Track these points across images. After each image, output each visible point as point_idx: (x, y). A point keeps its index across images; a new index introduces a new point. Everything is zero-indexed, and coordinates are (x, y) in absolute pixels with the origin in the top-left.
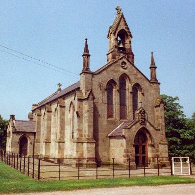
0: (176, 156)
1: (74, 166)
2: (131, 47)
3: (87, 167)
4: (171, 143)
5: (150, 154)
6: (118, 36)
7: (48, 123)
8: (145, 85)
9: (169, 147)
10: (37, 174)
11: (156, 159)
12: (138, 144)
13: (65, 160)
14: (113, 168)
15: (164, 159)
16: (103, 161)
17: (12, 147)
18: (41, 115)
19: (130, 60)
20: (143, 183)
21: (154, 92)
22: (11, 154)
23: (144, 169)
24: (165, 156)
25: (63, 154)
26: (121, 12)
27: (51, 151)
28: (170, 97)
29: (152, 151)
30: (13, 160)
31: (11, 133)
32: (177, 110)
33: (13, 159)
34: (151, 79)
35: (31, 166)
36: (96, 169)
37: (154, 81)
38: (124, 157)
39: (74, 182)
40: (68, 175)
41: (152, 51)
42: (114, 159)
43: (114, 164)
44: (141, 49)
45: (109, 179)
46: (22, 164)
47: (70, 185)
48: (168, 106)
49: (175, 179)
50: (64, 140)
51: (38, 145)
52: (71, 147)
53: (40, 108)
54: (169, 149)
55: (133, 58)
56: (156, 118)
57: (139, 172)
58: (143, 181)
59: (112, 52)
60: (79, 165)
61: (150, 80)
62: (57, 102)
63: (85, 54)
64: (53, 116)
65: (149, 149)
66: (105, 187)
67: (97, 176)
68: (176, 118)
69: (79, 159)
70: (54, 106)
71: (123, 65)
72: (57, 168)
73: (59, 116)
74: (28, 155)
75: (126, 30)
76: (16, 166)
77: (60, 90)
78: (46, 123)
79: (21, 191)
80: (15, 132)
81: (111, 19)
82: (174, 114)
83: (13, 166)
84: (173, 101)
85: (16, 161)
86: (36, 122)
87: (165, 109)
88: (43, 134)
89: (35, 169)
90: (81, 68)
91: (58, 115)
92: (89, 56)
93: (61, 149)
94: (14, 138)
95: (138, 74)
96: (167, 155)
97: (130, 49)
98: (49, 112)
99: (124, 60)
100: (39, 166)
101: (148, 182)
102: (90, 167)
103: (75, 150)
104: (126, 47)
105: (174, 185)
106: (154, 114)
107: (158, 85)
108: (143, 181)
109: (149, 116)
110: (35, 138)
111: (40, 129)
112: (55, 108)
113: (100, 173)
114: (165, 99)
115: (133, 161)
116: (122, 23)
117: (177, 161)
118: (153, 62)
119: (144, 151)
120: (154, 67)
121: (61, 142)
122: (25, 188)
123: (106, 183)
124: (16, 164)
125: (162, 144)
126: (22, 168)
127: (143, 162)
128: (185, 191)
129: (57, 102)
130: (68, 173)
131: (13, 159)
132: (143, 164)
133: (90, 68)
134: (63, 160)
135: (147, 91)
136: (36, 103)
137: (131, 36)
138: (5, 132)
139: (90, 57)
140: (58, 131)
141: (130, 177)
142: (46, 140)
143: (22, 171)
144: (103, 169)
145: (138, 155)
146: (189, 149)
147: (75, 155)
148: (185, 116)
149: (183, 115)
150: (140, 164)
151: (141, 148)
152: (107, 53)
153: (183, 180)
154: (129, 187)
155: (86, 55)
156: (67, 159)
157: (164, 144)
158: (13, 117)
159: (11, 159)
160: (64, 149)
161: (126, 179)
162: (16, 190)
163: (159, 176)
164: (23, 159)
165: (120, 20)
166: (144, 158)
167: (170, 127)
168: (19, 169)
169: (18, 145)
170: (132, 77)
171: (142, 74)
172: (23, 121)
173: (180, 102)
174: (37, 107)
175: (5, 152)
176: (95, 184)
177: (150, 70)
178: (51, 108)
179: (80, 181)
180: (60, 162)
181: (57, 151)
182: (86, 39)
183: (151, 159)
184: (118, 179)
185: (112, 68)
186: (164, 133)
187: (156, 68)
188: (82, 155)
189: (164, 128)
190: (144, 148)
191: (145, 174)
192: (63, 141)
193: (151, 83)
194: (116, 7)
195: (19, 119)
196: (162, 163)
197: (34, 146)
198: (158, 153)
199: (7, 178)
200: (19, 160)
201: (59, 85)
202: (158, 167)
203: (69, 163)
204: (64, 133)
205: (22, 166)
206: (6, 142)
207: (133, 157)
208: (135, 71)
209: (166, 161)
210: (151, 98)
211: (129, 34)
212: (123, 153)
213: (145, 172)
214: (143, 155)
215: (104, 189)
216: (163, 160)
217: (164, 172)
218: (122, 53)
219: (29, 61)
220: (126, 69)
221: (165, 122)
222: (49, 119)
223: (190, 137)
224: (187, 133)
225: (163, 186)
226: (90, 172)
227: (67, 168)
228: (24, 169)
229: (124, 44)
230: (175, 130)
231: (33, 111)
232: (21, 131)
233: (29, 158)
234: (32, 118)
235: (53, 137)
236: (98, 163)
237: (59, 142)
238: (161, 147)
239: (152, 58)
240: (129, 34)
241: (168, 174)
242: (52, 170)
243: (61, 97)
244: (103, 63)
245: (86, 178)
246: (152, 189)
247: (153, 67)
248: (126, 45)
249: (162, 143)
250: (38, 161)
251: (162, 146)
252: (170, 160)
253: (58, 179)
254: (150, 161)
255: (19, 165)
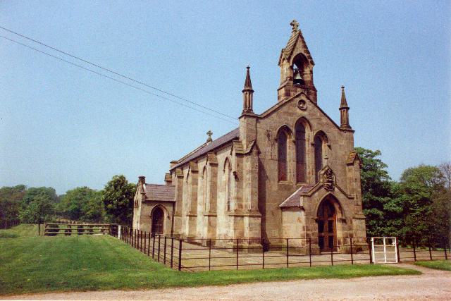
0: (377, 236)
1: (231, 250)
2: (312, 78)
3: (249, 252)
4: (369, 218)
5: (339, 233)
6: (293, 63)
7: (193, 189)
8: (332, 133)
9: (367, 222)
10: (178, 262)
11: (349, 240)
12: (322, 219)
13: (217, 241)
14: (286, 252)
15: (360, 240)
16: (273, 242)
17: (141, 223)
18: (183, 177)
19: (311, 97)
20: (329, 274)
21: (346, 144)
22: (140, 233)
23: (332, 254)
24: (361, 236)
25: (214, 233)
26: (299, 28)
27: (197, 229)
28: (368, 151)
29: (343, 229)
30: (143, 242)
31: (140, 203)
32: (378, 169)
33: (143, 240)
34: (341, 125)
35: (169, 249)
36: (262, 255)
37: (346, 128)
38: (303, 237)
39: (230, 273)
40: (221, 264)
41: (343, 84)
42: (287, 239)
43: (288, 248)
44: (327, 82)
45: (281, 269)
46: (155, 247)
47: (224, 278)
48: (366, 164)
49: (375, 269)
50: (216, 211)
51: (179, 219)
52: (225, 223)
53: (182, 167)
54: (366, 226)
55: (316, 95)
56: (347, 181)
57: (324, 259)
58: (330, 272)
59: (285, 86)
60: (238, 249)
61: (339, 126)
62: (206, 158)
63: (247, 89)
64: (200, 179)
65: (339, 225)
66: (275, 281)
67: (263, 264)
68: (377, 181)
69: (238, 241)
70: (202, 164)
71: (301, 105)
72: (206, 253)
73: (209, 178)
74: (164, 234)
75: (306, 55)
76: (147, 250)
77: (210, 140)
78: (190, 188)
79: (155, 286)
80: (146, 202)
81: (284, 38)
82: (375, 176)
83: (143, 250)
84: (373, 157)
85: (147, 243)
86: (176, 187)
87: (361, 167)
88: (186, 205)
89: (174, 255)
90: (240, 109)
91: (207, 176)
92: (252, 91)
93: (212, 226)
94: (145, 209)
95: (322, 118)
96: (364, 235)
97: (311, 82)
98: (195, 172)
99: (303, 98)
100: (180, 250)
101: (337, 273)
102: (253, 251)
103: (232, 228)
104: (305, 79)
105: (374, 278)
106: (345, 175)
107: (351, 133)
108: (330, 272)
109: (338, 178)
110: (174, 210)
111: (182, 197)
112: (203, 167)
113: (267, 260)
114: (361, 153)
115: (316, 243)
116: (300, 45)
117: (378, 244)
118: (344, 101)
119: (331, 229)
120: (345, 108)
121: (212, 215)
122: (159, 282)
123: (277, 275)
124: (147, 247)
125: (357, 218)
126: (156, 254)
127: (329, 244)
128: (391, 286)
129: (206, 158)
130: (222, 260)
131: (143, 240)
132: (329, 247)
133: (253, 109)
134: (214, 242)
135: (336, 142)
136: (177, 159)
137: (313, 63)
138: (132, 200)
139: (254, 94)
140: (208, 200)
141: (311, 266)
142: (190, 212)
143: (156, 257)
144: (273, 255)
145: (323, 234)
146: (395, 226)
147: (232, 234)
148: (391, 179)
149: (387, 177)
150: (326, 248)
151: (326, 224)
152: (278, 87)
153: (387, 271)
154: (310, 280)
155: (248, 90)
156: (221, 241)
157: (360, 219)
158: (142, 179)
159: (140, 240)
160: (216, 225)
161: (305, 269)
162: (147, 284)
163: (353, 265)
164: (157, 240)
165: (297, 40)
166: (332, 239)
167: (369, 194)
168: (151, 255)
169: (150, 220)
170: (314, 123)
171: (328, 117)
172: (157, 186)
173: (383, 158)
174: (177, 165)
175: (132, 230)
176: (261, 276)
177: (339, 112)
178: (197, 167)
179: (239, 272)
180: (210, 244)
181: (206, 229)
182: (248, 68)
183: (342, 241)
184: (293, 268)
185: (285, 109)
186: (360, 203)
187: (348, 109)
188: (242, 234)
189: (359, 195)
190: (331, 224)
191: (332, 261)
192: (215, 214)
193: (341, 130)
194: (291, 22)
195: (152, 183)
196: (357, 246)
197: (173, 221)
198: (351, 232)
199: (134, 267)
200: (152, 242)
201: (210, 133)
202: (351, 251)
203: (223, 246)
204: (216, 202)
205: (155, 251)
206: (132, 216)
207: (315, 237)
208: (319, 114)
209: (363, 243)
210: (340, 152)
211: (310, 60)
212: (301, 232)
213: (332, 259)
214: (331, 234)
215: (274, 283)
216: (358, 241)
217: (360, 258)
218: (299, 87)
219: (166, 99)
220: (305, 110)
221: (361, 186)
222: (195, 182)
223: (398, 208)
224: (393, 203)
225: (359, 279)
226: (254, 259)
227: (221, 253)
228: (159, 254)
229: (302, 75)
230: (375, 198)
231: (172, 171)
232: (154, 199)
233: (166, 238)
234: (171, 182)
235: (200, 209)
236: (265, 245)
237: (209, 216)
238: (355, 223)
239: (343, 94)
240: (310, 60)
241: (365, 262)
242: (199, 256)
243: (211, 151)
244: (272, 101)
245: (247, 267)
246: (342, 283)
247: (344, 108)
248: (305, 75)
249: (357, 216)
250: (178, 242)
251: (357, 221)
252: (368, 241)
253: (207, 269)
254: (339, 243)
255: (151, 249)
